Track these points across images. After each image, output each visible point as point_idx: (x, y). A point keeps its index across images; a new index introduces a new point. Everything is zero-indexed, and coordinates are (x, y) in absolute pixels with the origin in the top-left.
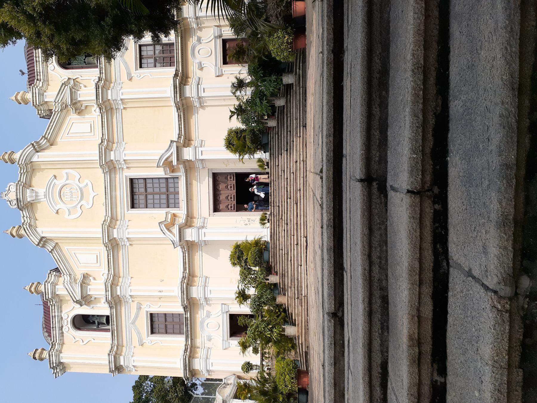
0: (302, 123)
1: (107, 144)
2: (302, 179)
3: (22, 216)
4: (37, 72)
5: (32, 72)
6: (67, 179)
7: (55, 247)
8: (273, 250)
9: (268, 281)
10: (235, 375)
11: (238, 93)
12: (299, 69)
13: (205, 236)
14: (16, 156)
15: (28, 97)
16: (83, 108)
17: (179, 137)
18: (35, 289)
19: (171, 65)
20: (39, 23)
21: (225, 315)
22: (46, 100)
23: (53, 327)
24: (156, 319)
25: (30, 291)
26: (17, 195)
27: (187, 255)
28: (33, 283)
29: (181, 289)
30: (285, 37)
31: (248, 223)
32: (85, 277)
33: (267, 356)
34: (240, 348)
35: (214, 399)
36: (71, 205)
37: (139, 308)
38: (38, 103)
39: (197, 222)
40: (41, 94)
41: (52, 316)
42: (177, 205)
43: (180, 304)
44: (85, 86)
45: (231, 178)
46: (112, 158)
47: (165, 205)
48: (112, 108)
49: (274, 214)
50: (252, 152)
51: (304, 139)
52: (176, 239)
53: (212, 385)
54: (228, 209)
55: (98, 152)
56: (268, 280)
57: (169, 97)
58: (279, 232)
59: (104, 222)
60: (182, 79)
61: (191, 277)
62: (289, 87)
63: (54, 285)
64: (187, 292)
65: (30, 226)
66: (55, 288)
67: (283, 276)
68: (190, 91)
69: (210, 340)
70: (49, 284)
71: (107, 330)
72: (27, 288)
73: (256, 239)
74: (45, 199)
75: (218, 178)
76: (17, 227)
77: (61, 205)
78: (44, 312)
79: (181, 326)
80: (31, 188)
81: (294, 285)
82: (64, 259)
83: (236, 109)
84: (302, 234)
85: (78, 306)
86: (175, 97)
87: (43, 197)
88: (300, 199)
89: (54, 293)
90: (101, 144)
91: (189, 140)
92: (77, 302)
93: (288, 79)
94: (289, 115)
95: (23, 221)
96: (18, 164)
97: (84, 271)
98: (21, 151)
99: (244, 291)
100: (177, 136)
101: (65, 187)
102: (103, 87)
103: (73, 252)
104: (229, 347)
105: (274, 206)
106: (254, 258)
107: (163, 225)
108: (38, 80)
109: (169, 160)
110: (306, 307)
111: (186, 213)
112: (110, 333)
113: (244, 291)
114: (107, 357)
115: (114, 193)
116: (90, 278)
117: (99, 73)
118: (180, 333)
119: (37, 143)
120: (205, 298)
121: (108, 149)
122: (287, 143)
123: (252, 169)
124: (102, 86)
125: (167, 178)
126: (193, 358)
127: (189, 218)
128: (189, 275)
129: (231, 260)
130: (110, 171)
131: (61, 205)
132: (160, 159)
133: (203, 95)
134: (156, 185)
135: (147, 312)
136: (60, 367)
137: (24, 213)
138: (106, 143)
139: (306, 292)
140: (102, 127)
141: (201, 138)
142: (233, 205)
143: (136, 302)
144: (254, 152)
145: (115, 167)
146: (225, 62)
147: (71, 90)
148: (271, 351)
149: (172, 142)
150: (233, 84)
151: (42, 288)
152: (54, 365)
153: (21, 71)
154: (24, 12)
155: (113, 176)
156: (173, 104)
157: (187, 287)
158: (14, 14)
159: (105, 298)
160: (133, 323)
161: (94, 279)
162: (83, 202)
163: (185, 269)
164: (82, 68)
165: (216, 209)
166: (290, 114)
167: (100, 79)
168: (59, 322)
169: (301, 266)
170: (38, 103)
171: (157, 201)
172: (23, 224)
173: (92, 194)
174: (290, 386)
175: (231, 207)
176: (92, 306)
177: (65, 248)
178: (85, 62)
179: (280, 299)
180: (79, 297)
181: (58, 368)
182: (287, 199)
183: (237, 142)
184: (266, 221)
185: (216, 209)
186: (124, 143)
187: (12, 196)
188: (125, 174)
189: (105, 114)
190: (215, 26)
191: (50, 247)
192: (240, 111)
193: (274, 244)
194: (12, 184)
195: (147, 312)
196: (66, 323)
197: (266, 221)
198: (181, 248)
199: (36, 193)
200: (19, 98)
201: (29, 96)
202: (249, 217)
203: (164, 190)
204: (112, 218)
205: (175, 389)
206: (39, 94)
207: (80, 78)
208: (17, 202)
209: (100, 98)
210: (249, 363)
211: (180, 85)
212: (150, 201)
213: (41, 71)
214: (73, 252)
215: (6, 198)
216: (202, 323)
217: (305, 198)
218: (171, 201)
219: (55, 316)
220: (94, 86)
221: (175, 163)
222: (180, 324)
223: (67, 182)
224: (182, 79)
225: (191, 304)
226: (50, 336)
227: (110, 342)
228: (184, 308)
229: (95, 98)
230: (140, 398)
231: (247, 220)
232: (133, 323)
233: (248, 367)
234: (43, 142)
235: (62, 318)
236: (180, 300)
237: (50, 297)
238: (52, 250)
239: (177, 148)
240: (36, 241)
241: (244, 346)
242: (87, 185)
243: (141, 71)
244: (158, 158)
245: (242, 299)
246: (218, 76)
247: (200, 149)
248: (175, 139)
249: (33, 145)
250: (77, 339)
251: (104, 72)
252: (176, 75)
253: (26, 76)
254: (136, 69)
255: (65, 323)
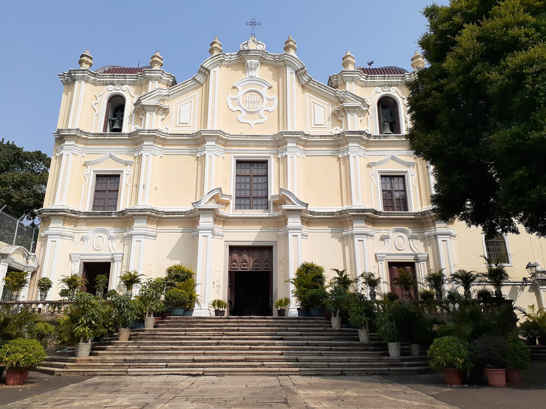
0: (346, 369)
1: (303, 140)
2: (277, 369)
3: (232, 54)
4: (374, 77)
5: (376, 72)
6: (268, 99)
7: (199, 82)
8: (184, 320)
9: (147, 315)
10: (38, 267)
11: (362, 280)
12: (408, 366)
13: (203, 236)
14: (292, 53)
15: (350, 67)
16: (339, 118)
17: (311, 213)
18: (156, 61)
19: (385, 207)
20: (461, 78)
21: (109, 257)
22: (347, 84)
23: (114, 75)
24: (113, 180)
25: (154, 57)
26: (253, 50)
27: (183, 216)
28: (162, 59)
29: (145, 209)
30: (461, 358)
31: (216, 285)
32: (166, 111)
33: (57, 309)
34: (69, 275)
35: (11, 243)
36: (239, 102)
37: (126, 164)
38: (344, 75)
39: (219, 229)
40: (353, 80)
41: (125, 76)
42: (239, 206)
43: (128, 207)
44: (361, 121)
45: (267, 266)
46: (289, 145)
47: (238, 195)
48: (339, 146)
49: (228, 322)
50: (300, 295)
51: (327, 373)
52: (202, 206)
53: (30, 239)
54: (232, 261)
55: (295, 130)
56: (149, 314)
57: (351, 204)
58: (206, 331)
59: (224, 132)
60: (370, 218)
61: (157, 219)
62: (383, 349)
63: (159, 79)
64: (141, 215)
65: (222, 61)
66: (156, 80)
67: (153, 336)
68: (359, 227)
69: (82, 239)
70: (160, 75)
71: (105, 129)
72: (158, 54)
73: (198, 297)
74: (248, 77)
75: (266, 251)
76: (221, 48)
77: (242, 91)
78: (130, 69)
79: (103, 208)
80: (259, 64)
81: (142, 354)
82: (184, 91)
83: (346, 276)
84: (207, 369)
85: (135, 102)
86: (353, 210)
87: (250, 75)
88: (251, 366)
89: (150, 78)
90: (304, 134)
91: (307, 222)
92: (139, 101)
93: (394, 349)
94: (350, 348)
95: (226, 54)
96: (285, 54)
97: (172, 110)
98: (297, 57)
99: (138, 281)
100: (312, 210)
101: (260, 96)
102: (361, 138)
103: (192, 100)
104: (72, 262)
105: (237, 322)
106: (175, 292)
107: (218, 192)
108: (367, 77)
109: (287, 201)
110: (113, 373)
111: (230, 216)
112: (101, 131)
113: (138, 281)
114: (75, 127)
115: (252, 144)
116: (164, 116)
117: (375, 135)
118: (94, 207)
119: (305, 73)
120: (132, 235)
121: (298, 141)
122: (316, 345)
123: (277, 291)
124: (361, 137)
125: (267, 197)
126: (64, 220)
127: (223, 219)
128: (160, 218)
129: (175, 267)
130: (275, 141)
131: (242, 91)
132: (289, 192)
133: (356, 239)
134: (260, 187)
135: (122, 171)
136: (70, 80)
137: (235, 56)
138: (304, 138)
139: (132, 374)
140: (320, 136)
141: (310, 235)
142: (236, 267)
143: (134, 161)
144: (300, 298)
145: (279, 146)
146: (391, 265)
147: (359, 107)
148: (61, 315)
149: (307, 205)
150: (373, 275)
151: (157, 67)
152: (73, 75)
153: (372, 62)
154: (474, 63)
155: (271, 144)
156: (345, 207)
157: (147, 215)
158: (472, 52)
159: (141, 128)
160: (111, 157)
161: (163, 119)
162: (244, 113)
163: (167, 213)
164: (379, 119)
165: (232, 249)
166: (351, 350)
167: (369, 136)
168: (118, 81)
169: (167, 366)
170: (344, 75)
171: (243, 187)
172: (224, 54)
173: (252, 123)
174: (7, 359)
175: (234, 266)
176: (134, 115)
177: (198, 93)
178: (384, 122)
179: (124, 334)
180: (144, 102)
181: (69, 78)
182: (249, 344)
183: (309, 276)
184: (217, 308)
185: (232, 249)
186: (304, 156)
187: (252, 46)
188: (272, 156)
189: (333, 139)
190: (428, 255)
191: (199, 78)
192: (343, 281)
193: (192, 322)
194: (265, 47)
195: (122, 171)
196: (116, 88)
197: (217, 308)
198: (192, 210)
199: (255, 69)
200: (349, 58)
201: (351, 68)
202: (222, 286)
203: (255, 194)
204: (227, 140)
205: (31, 196)
206: (353, 77)
207: (369, 117)
208: (247, 50)
209: (350, 135)
210: (50, 286)
211: (366, 215)
212: (243, 180)
213: (375, 80)
214: (192, 100)
215: (250, 40)
216: (105, 232)
217: (254, 373)
218: (243, 201)
219: (126, 78)
220: (361, 130)
221: (285, 207)
222: (104, 207)
223: (265, 99)
224: (370, 218)
225: (127, 219)
226: (105, 72)
227: (92, 132)
228: (122, 212)
229: (350, 129)
230: (26, 159)
231: (218, 284)
232: (111, 157)
233: (45, 285)
234: (306, 79)
235: (123, 85)
236: (132, 207)
237: (146, 74)
238: (196, 80)
239: (301, 210)
240: (206, 65)
241: (71, 282)
242: (262, 118)
243: (378, 176)
244: (289, 189)
245: (128, 279)
246: (376, 256)
247: (299, 235)
248: (310, 208)
249: (303, 68)
250: (98, 98)
251: (376, 139)
252: (375, 212)
253: (368, 67)
254: (379, 172)
255: (116, 87)
